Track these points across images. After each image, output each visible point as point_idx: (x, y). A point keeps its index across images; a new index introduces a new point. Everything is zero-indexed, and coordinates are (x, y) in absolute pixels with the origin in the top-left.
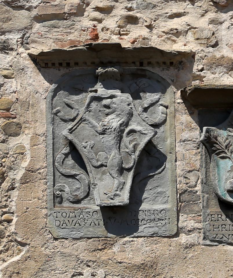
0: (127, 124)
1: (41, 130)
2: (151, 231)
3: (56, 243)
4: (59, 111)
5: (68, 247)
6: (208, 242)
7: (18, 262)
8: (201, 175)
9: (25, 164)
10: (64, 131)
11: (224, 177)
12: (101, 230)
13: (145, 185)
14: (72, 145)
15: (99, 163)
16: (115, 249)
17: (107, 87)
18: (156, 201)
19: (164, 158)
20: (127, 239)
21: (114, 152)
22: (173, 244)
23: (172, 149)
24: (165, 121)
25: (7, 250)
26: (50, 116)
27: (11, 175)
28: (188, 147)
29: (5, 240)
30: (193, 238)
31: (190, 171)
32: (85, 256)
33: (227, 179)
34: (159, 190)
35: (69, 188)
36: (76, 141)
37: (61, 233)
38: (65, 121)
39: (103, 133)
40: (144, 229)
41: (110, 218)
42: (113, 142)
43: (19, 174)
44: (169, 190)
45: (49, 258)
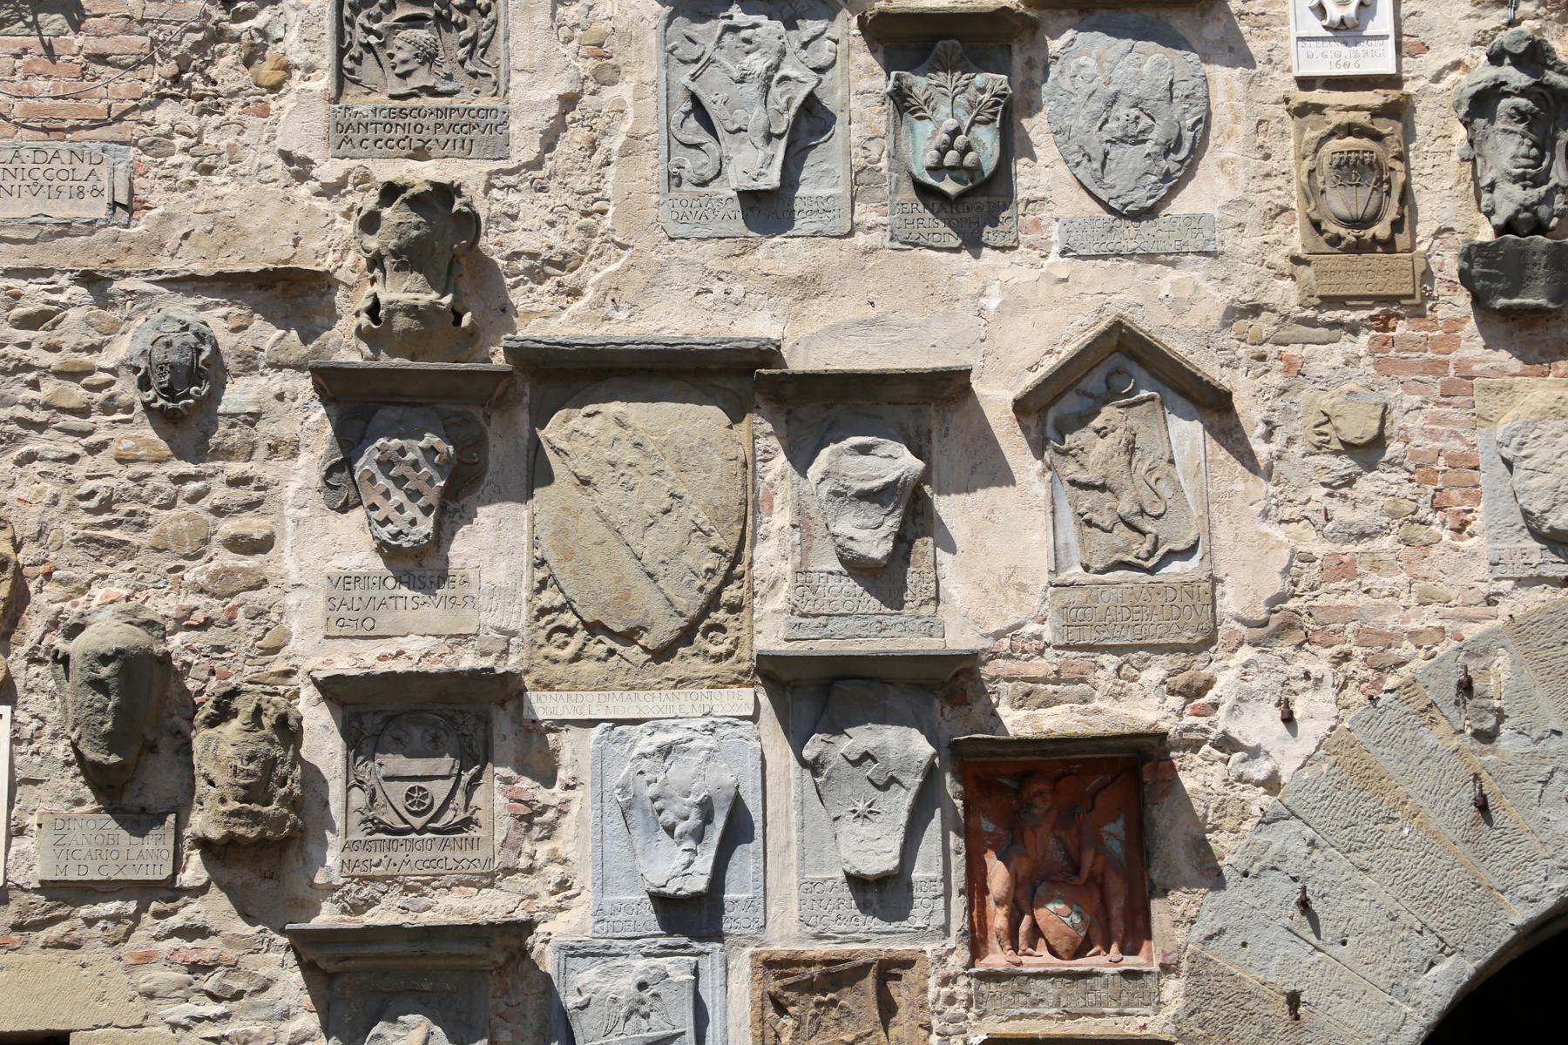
0: (777, 68)
1: (649, 76)
2: (814, 227)
3: (673, 245)
4: (675, 48)
5: (689, 251)
6: (897, 245)
7: (616, 273)
8: (888, 144)
9: (626, 127)
10: (683, 76)
11: (922, 148)
12: (739, 227)
13: (804, 158)
14: (694, 98)
15: (736, 126)
16: (760, 254)
17: (747, 11)
18: (822, 181)
19: (833, 118)
20: (777, 239)
21: (758, 109)
22: (846, 248)
23: (845, 105)
24: (834, 62)
25: (601, 255)
26: (663, 55)
27: (605, 143)
28: (868, 102)
29: (598, 240)
30: (875, 239)
31: (871, 139)
32: (715, 265)
33: (926, 151)
34: (825, 166)
35: (692, 164)
36: (700, 93)
37: (681, 230)
38: (685, 62)
39: (741, 81)
40: (802, 224)
41: (751, 209)
42: (756, 94)
43: (616, 143)
44: (840, 169)
45: (662, 267)
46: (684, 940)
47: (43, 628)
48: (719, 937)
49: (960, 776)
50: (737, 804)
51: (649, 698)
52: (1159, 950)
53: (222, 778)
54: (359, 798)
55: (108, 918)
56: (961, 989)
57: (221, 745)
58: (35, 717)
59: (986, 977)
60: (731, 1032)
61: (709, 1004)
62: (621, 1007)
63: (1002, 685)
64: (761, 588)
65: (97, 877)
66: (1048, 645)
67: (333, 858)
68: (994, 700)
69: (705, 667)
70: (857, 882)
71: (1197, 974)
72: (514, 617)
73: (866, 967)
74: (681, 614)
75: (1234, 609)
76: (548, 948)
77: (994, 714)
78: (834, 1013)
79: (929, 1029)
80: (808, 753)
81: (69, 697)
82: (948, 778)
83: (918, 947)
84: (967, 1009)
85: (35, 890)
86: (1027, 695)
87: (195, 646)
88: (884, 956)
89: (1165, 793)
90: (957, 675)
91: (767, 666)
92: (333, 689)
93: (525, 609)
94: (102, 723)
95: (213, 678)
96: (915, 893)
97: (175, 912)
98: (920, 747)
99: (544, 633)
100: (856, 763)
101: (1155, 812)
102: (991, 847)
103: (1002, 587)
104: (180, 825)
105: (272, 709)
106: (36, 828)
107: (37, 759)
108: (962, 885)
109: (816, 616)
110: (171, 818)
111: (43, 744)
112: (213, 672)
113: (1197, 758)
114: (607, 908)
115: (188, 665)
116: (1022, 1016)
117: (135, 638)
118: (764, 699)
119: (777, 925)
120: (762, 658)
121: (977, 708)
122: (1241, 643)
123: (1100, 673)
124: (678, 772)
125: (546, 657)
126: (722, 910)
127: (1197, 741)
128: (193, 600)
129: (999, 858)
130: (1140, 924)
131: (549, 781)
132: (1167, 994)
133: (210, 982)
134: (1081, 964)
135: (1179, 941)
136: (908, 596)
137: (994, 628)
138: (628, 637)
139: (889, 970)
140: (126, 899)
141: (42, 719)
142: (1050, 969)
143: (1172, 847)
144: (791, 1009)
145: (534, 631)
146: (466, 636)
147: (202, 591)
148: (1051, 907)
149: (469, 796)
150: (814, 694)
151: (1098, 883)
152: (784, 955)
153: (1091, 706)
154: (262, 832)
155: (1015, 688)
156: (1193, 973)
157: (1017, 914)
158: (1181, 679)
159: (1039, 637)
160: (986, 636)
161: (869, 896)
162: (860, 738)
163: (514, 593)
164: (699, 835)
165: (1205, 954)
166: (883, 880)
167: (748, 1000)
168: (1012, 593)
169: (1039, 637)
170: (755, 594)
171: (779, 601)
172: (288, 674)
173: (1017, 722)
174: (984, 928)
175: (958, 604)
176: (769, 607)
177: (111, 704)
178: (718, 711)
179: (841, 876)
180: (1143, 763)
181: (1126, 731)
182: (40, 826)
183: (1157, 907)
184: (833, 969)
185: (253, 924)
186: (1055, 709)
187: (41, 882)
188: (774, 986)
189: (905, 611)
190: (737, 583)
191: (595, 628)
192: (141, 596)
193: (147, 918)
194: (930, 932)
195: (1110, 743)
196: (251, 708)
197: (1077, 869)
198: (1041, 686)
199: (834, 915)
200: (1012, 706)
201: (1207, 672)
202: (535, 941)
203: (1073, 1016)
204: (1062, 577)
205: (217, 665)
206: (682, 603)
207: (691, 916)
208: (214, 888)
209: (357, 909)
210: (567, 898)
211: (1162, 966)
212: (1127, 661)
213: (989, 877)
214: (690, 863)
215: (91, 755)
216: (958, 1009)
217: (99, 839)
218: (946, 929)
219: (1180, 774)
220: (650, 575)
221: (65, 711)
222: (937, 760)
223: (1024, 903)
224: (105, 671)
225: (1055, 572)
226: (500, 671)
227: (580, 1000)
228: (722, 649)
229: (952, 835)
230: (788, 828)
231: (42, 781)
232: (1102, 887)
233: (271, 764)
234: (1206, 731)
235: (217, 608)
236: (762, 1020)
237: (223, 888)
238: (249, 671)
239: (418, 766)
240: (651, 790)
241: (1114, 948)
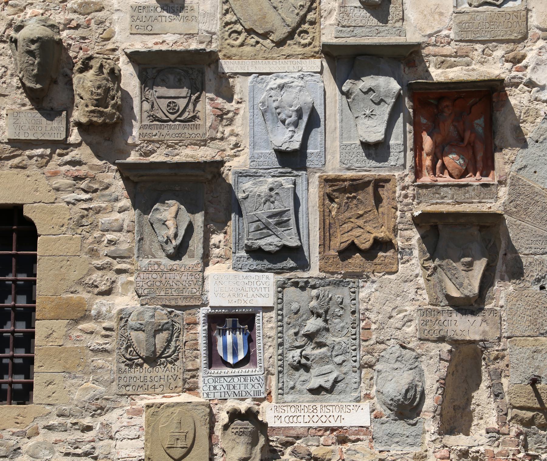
46: (290, 170)
47: (5, 27)
48: (305, 168)
49: (411, 99)
50: (313, 112)
51: (274, 63)
52: (498, 175)
53: (86, 96)
54: (146, 106)
55: (38, 156)
57: (86, 81)
58: (3, 66)
59: (421, 186)
60: (310, 210)
61: (300, 197)
62: (262, 199)
63: (431, 58)
64: (324, 14)
65: (33, 138)
66: (452, 40)
67: (135, 132)
68: (427, 65)
69: (299, 50)
70: (365, 145)
71: (514, 185)
72: (214, 26)
73: (369, 182)
74: (288, 26)
75: (536, 23)
76: (230, 173)
77: (427, 71)
78: (355, 202)
80: (344, 89)
81: (18, 58)
82: (406, 99)
83: (392, 174)
84: (413, 200)
85: (6, 143)
86: (442, 62)
87: (73, 36)
88: (377, 177)
89: (503, 106)
90: (411, 53)
91: (327, 49)
92: (134, 57)
93: (219, 23)
94: (33, 70)
95: (81, 51)
96: (391, 150)
97: (67, 154)
98: (394, 86)
99: (227, 33)
100: (366, 93)
101: (498, 114)
102: (425, 130)
103: (432, 14)
104: (68, 116)
105: (107, 66)
106: (5, 116)
107: (5, 86)
108: (412, 147)
109: (349, 27)
110: (64, 113)
111: (7, 79)
112: (81, 49)
113: (517, 91)
114: (256, 156)
115: (70, 45)
116: (437, 203)
117: (45, 32)
118: (325, 64)
119: (330, 164)
120: (325, 46)
121: (420, 68)
122: (538, 39)
123: (475, 53)
124: (287, 96)
125: (229, 45)
126: (306, 157)
127: (517, 83)
128: (71, 16)
129: (428, 135)
130: (490, 164)
131: (230, 99)
132: (500, 194)
133: (83, 185)
134: (463, 181)
135: (507, 171)
136: (390, 18)
137: (428, 32)
138: (265, 36)
139: (380, 183)
140: (46, 148)
141: (6, 68)
142: (449, 183)
143: (505, 129)
144: (336, 200)
145: (223, 33)
146: (193, 34)
147: (75, 12)
148: (451, 156)
149: (195, 106)
150: (348, 62)
151: (472, 146)
153: (470, 67)
154: (105, 120)
155: (437, 59)
156: (512, 185)
157: (435, 159)
158: (511, 55)
159: (448, 36)
160: (425, 36)
161: (370, 152)
162: (368, 82)
163: (214, 15)
164: (296, 124)
165: (518, 176)
166: (377, 145)
167: (317, 196)
168: (437, 17)
169: (448, 36)
170: (321, 17)
171: (332, 20)
172: (114, 50)
173: (438, 74)
174: (421, 165)
175: (412, 22)
176: (328, 22)
177: (36, 62)
178: (305, 69)
179: (358, 142)
180: (493, 93)
181: (486, 78)
182: (7, 115)
183: (497, 156)
184: (355, 183)
185: (101, 160)
186: (455, 69)
187: (9, 139)
188: (329, 190)
189: (389, 25)
190: (314, 12)
191: (250, 32)
192: (48, 13)
193: (55, 157)
194: (397, 168)
195: (479, 84)
196: (98, 65)
197: (462, 139)
198: (448, 59)
199: (355, 160)
200: (436, 67)
201: (523, 51)
202: (224, 169)
203: (459, 203)
204: (459, 9)
205: (83, 45)
206: (289, 20)
207: (292, 160)
208: (84, 144)
209: (147, 154)
210: (238, 151)
211: (499, 181)
212: (488, 47)
213: (424, 143)
214: (292, 136)
215: (28, 84)
216: (409, 200)
217: (33, 121)
218: (404, 166)
219: (509, 97)
220: (275, 8)
221: (16, 64)
222: (402, 92)
223: (439, 155)
224: (33, 47)
225: (456, 7)
226: (208, 50)
227: (244, 195)
228: (306, 41)
229: (408, 125)
230: (335, 122)
231: (7, 95)
232: (473, 148)
233: (107, 90)
234: (521, 78)
235: (82, 20)
236: (324, 205)
237: (88, 144)
238: (97, 48)
239: (172, 92)
240: (275, 104)
241: (478, 174)
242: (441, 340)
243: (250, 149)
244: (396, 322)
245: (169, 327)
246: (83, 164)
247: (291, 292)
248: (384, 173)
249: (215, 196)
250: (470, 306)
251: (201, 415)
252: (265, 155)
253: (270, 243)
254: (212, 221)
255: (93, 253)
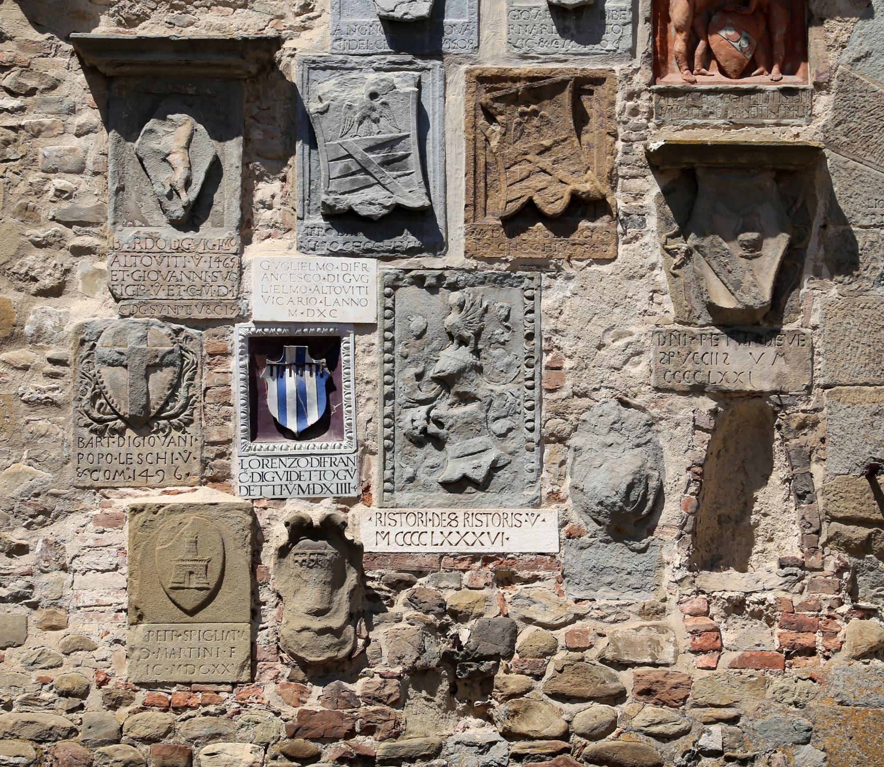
46: (409, 58)
48: (438, 55)
52: (813, 70)
56: (643, 103)
59: (666, 93)
60: (448, 136)
61: (430, 112)
62: (355, 113)
71: (845, 91)
73: (563, 84)
76: (293, 62)
78: (536, 121)
79: (615, 136)
83: (608, 67)
84: (648, 119)
88: (579, 74)
96: (607, 21)
108: (648, 14)
114: (344, 29)
116: (694, 126)
119: (489, 46)
126: (442, 33)
132: (818, 108)
134: (747, 83)
139: (584, 85)
142: (720, 86)
144: (499, 118)
148: (723, 33)
151: (765, 14)
152: (494, 72)
156: (841, 90)
157: (693, 39)
161: (567, 23)
165: (853, 74)
167: (463, 110)
174: (665, 51)
183: (814, 33)
184: (536, 84)
185: (43, 32)
199: (537, 39)
202: (282, 55)
203: (737, 126)
209: (131, 22)
210: (309, 19)
211: (815, 84)
213: (671, 8)
216: (641, 120)
218: (632, 52)
223: (700, 30)
227: (321, 106)
232: (768, 17)
236: (475, 127)
241: (775, 69)
242: (698, 390)
243: (333, 14)
244: (612, 353)
245: (176, 361)
246: (7, 38)
247: (409, 296)
248: (593, 66)
249: (264, 107)
250: (751, 326)
251: (235, 529)
252: (360, 27)
253: (370, 200)
254: (258, 155)
255: (27, 213)
